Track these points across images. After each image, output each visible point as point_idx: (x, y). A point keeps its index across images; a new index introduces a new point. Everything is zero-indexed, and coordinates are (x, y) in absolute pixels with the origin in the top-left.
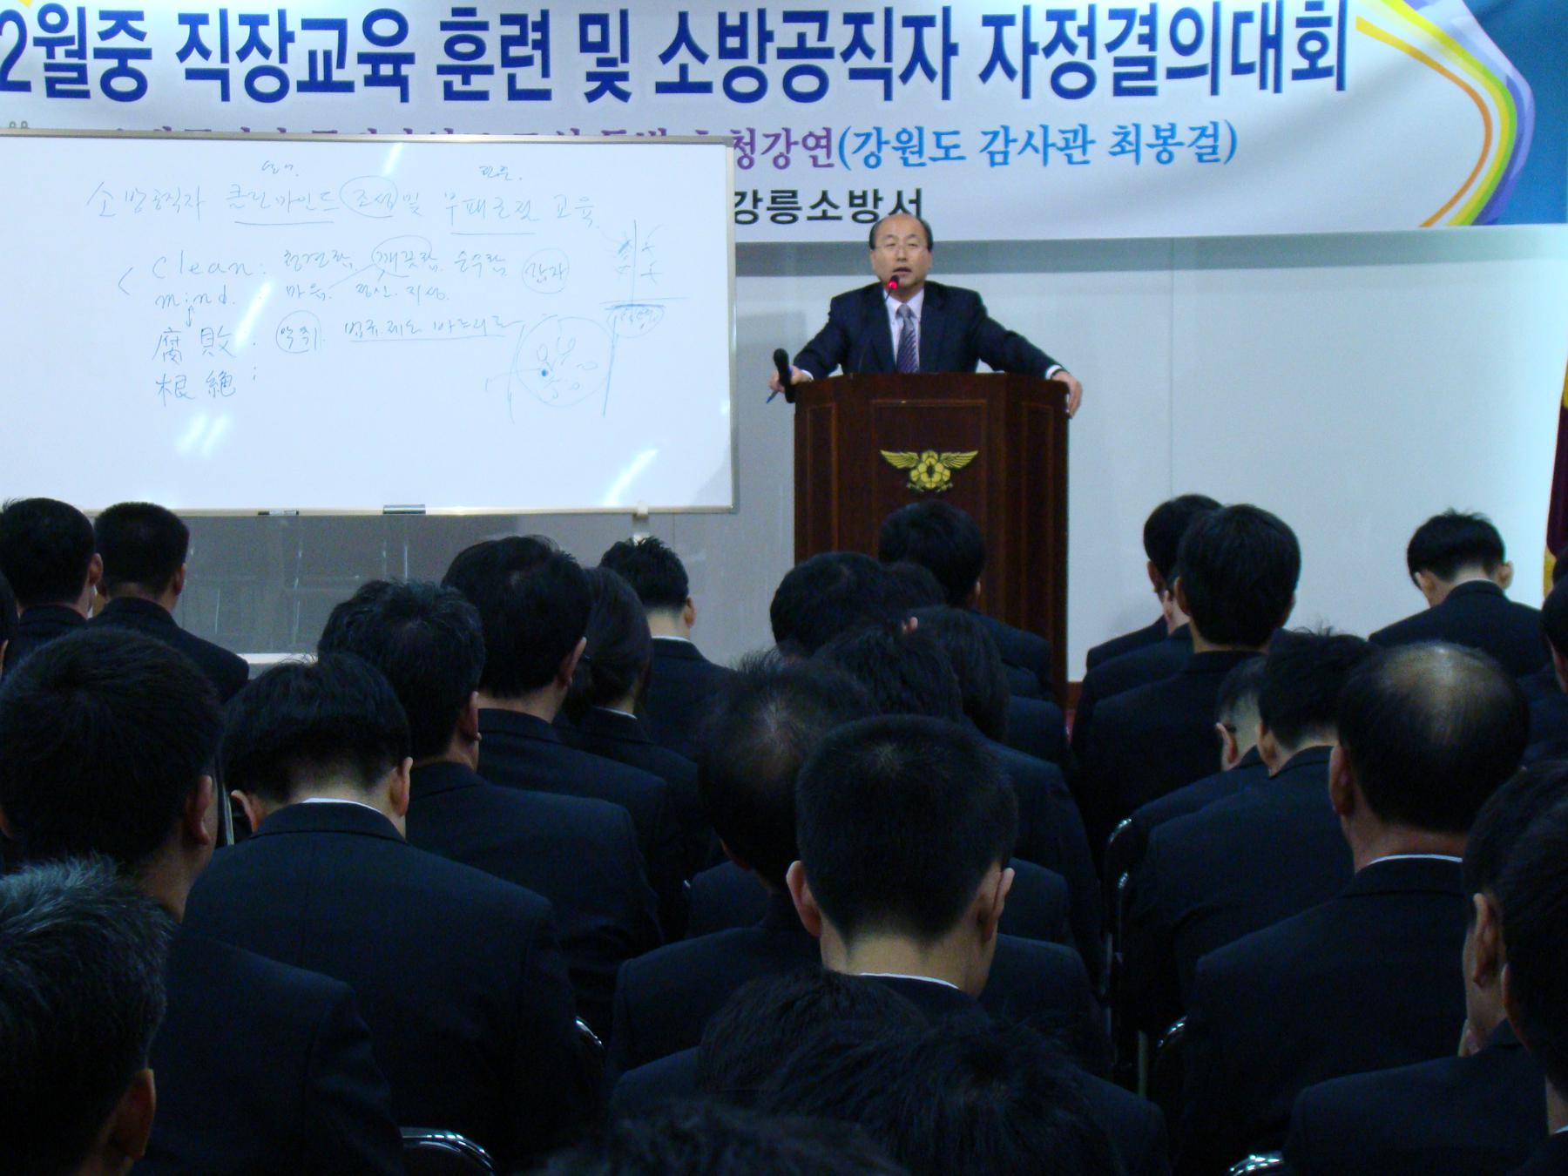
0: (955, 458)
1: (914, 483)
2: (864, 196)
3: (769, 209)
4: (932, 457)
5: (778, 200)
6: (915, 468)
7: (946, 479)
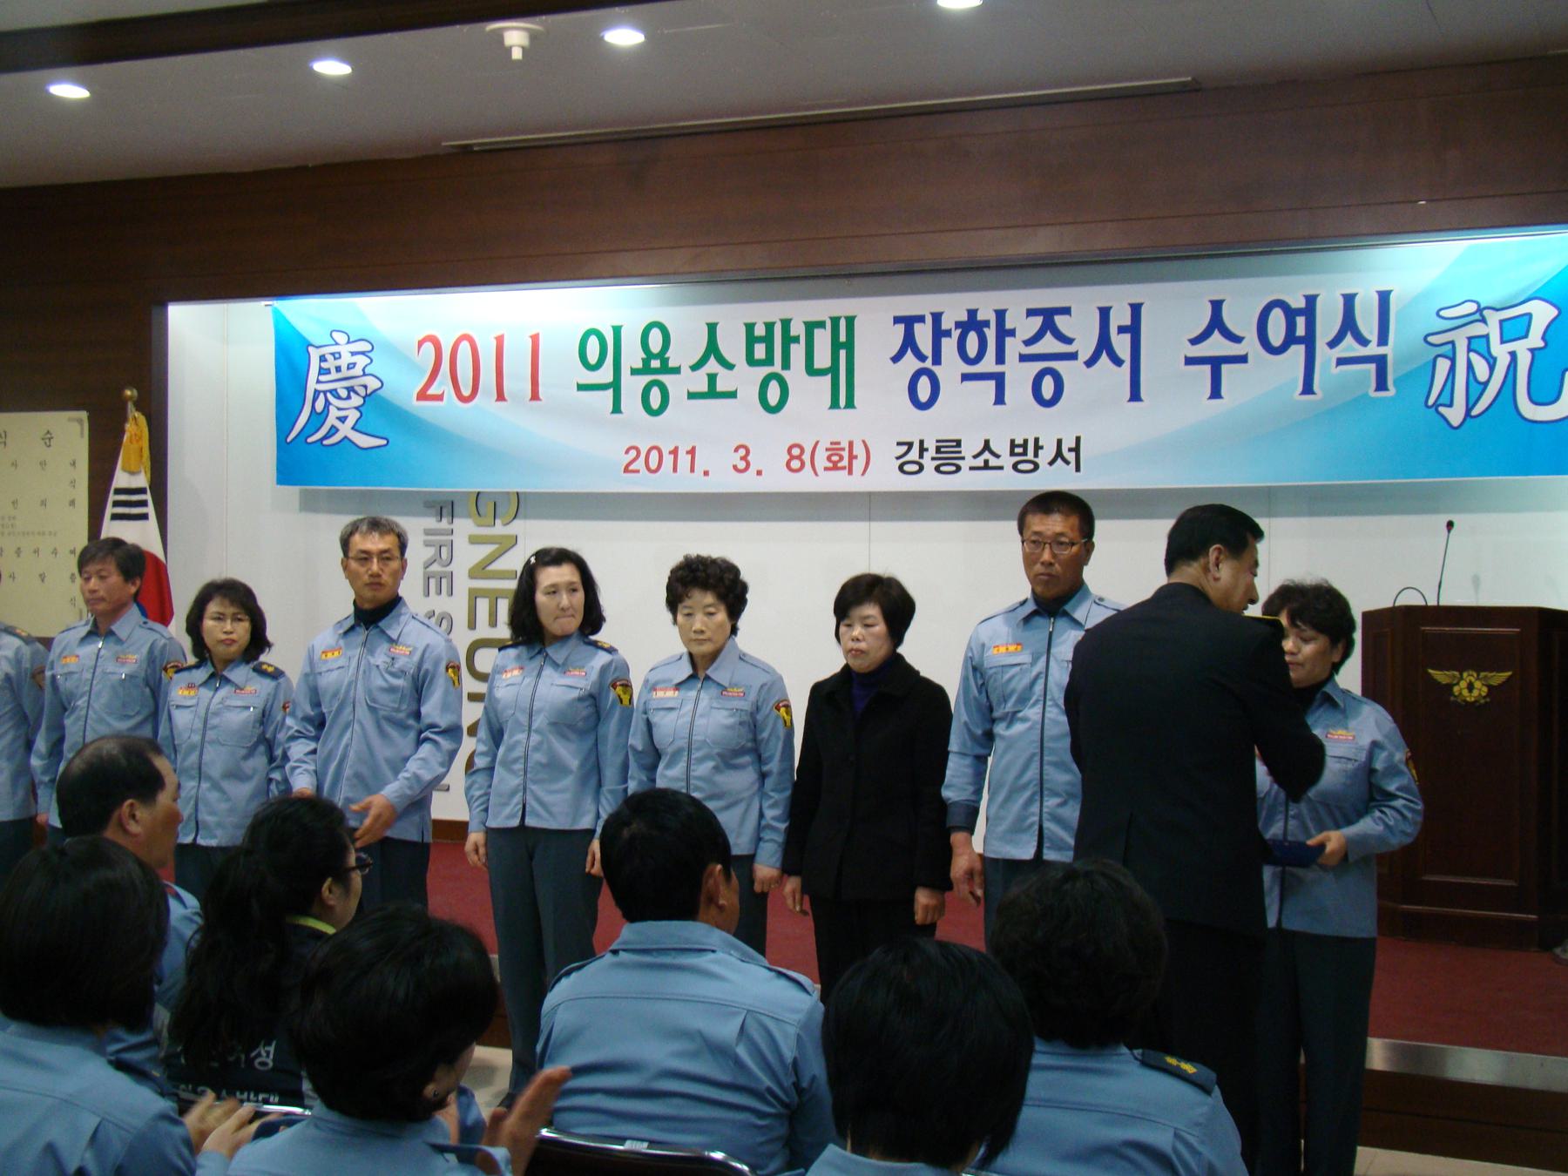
2: (1025, 444)
3: (933, 459)
5: (943, 450)
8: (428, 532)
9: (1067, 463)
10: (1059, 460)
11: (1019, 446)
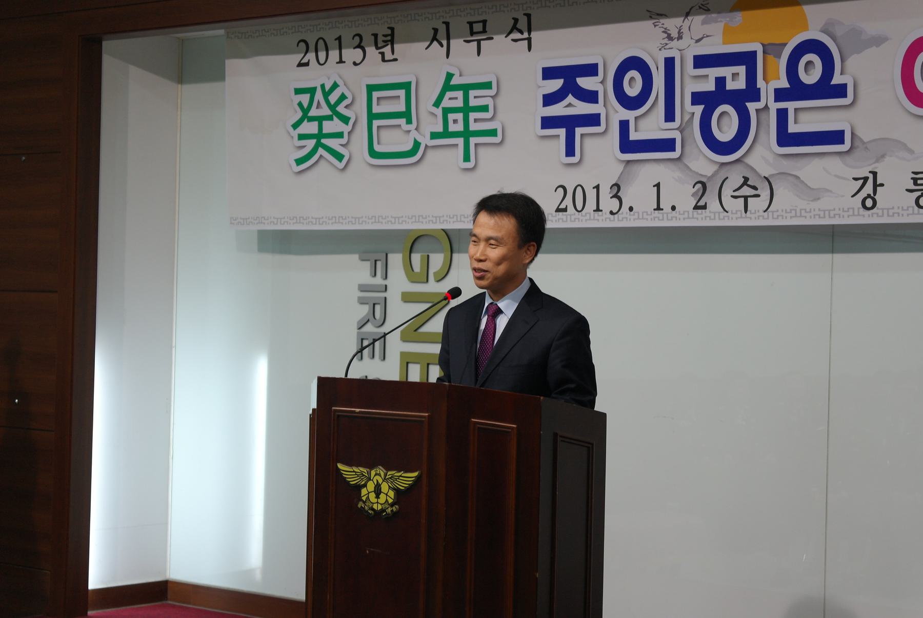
1: (364, 502)
4: (380, 475)
6: (365, 486)
7: (390, 501)
8: (363, 288)
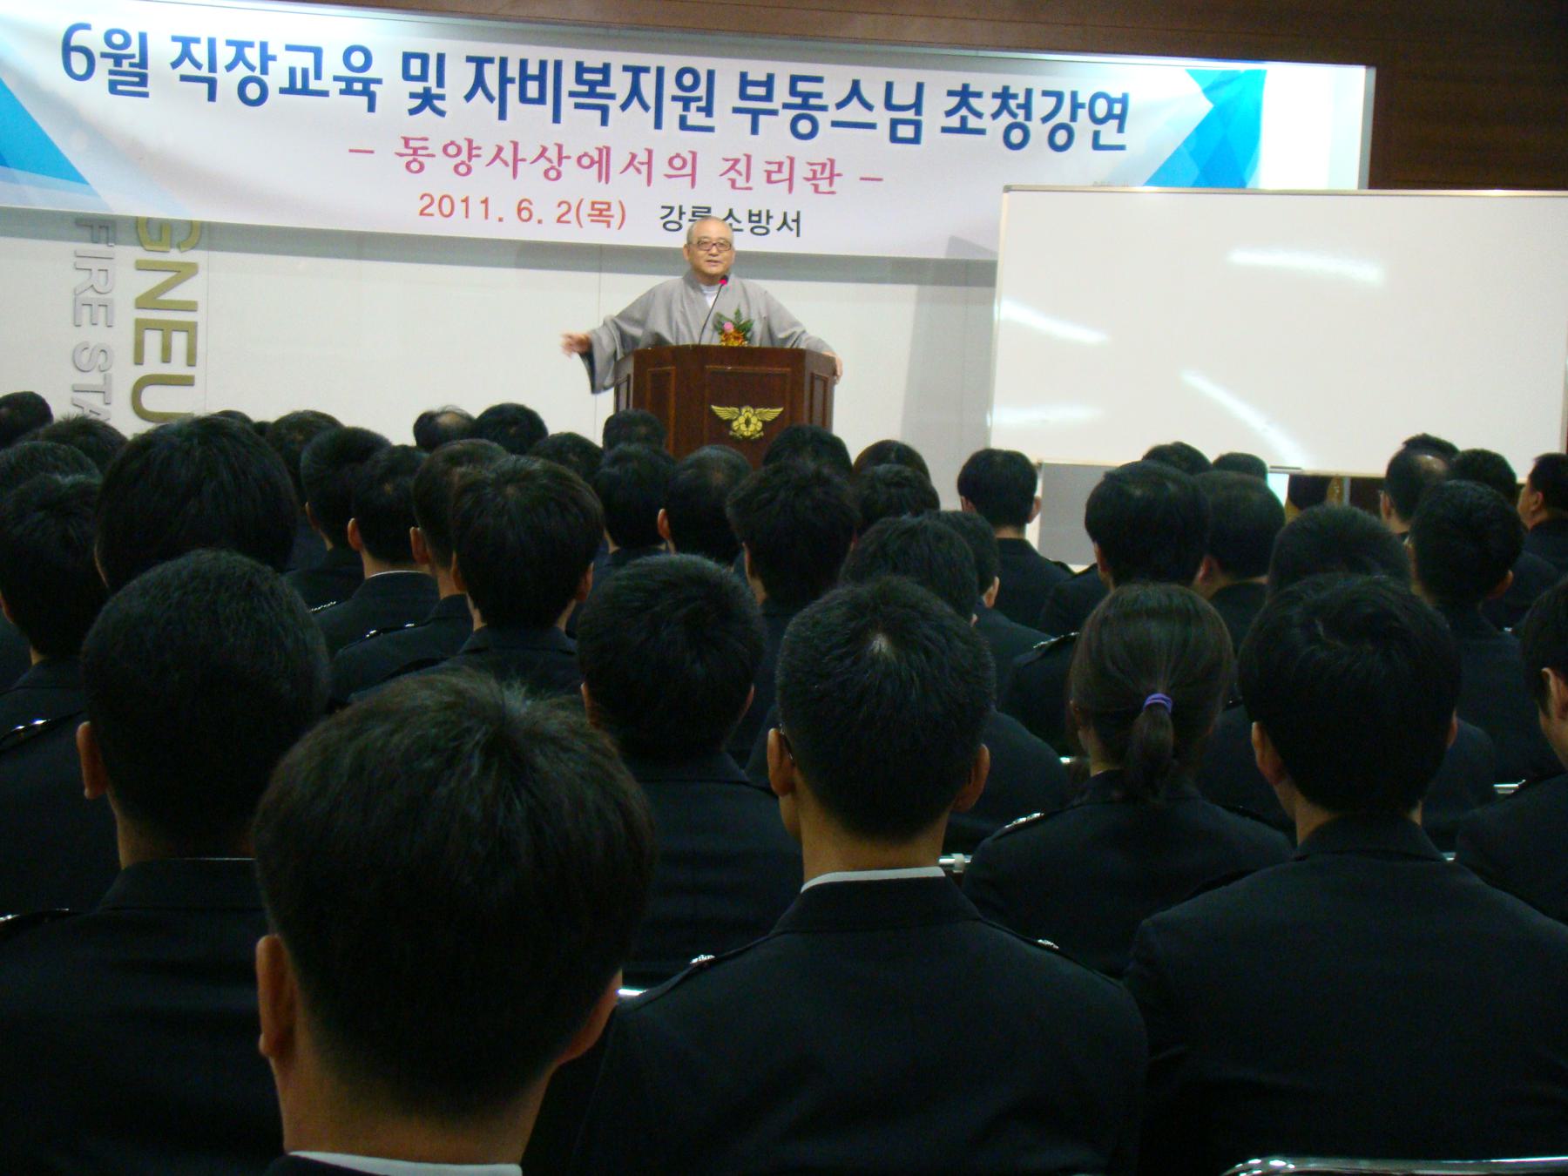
0: (766, 413)
1: (734, 431)
2: (759, 215)
5: (697, 214)
7: (759, 429)
9: (791, 229)
10: (785, 227)
11: (754, 215)
